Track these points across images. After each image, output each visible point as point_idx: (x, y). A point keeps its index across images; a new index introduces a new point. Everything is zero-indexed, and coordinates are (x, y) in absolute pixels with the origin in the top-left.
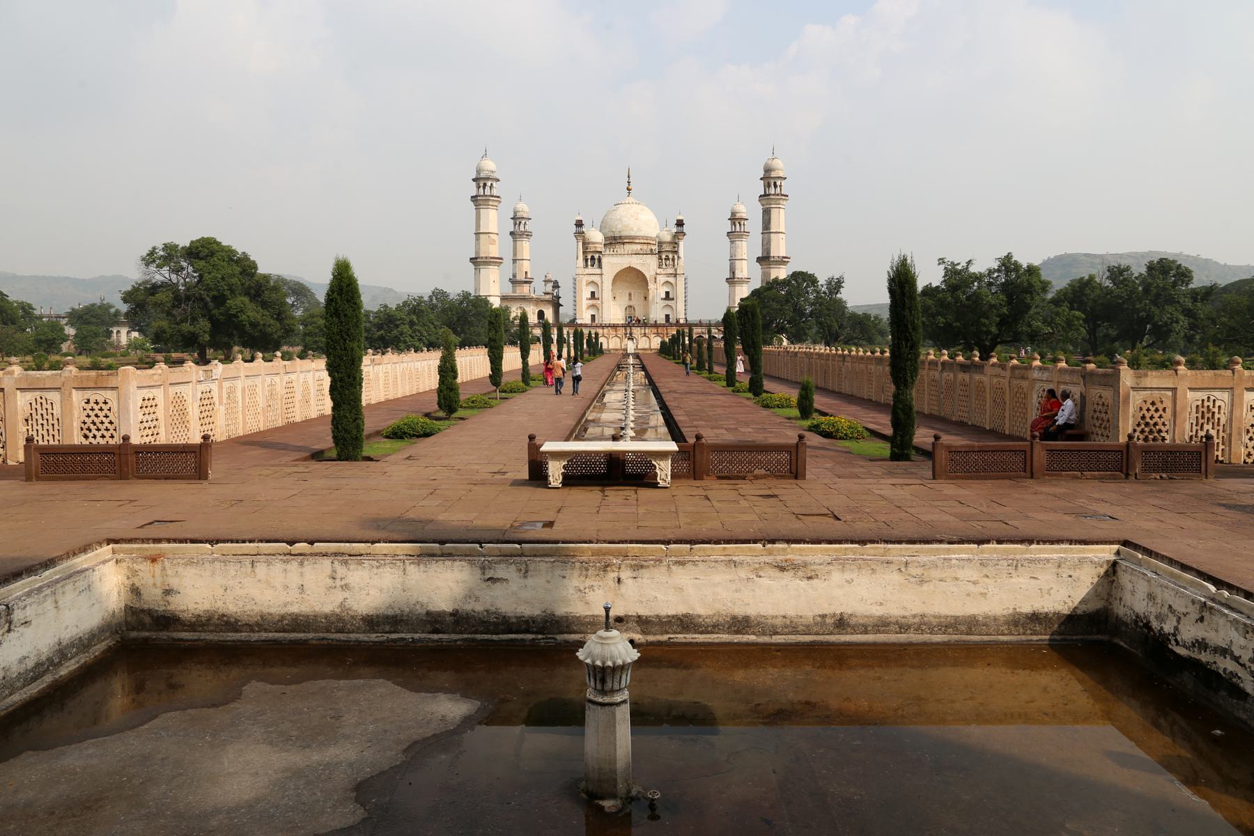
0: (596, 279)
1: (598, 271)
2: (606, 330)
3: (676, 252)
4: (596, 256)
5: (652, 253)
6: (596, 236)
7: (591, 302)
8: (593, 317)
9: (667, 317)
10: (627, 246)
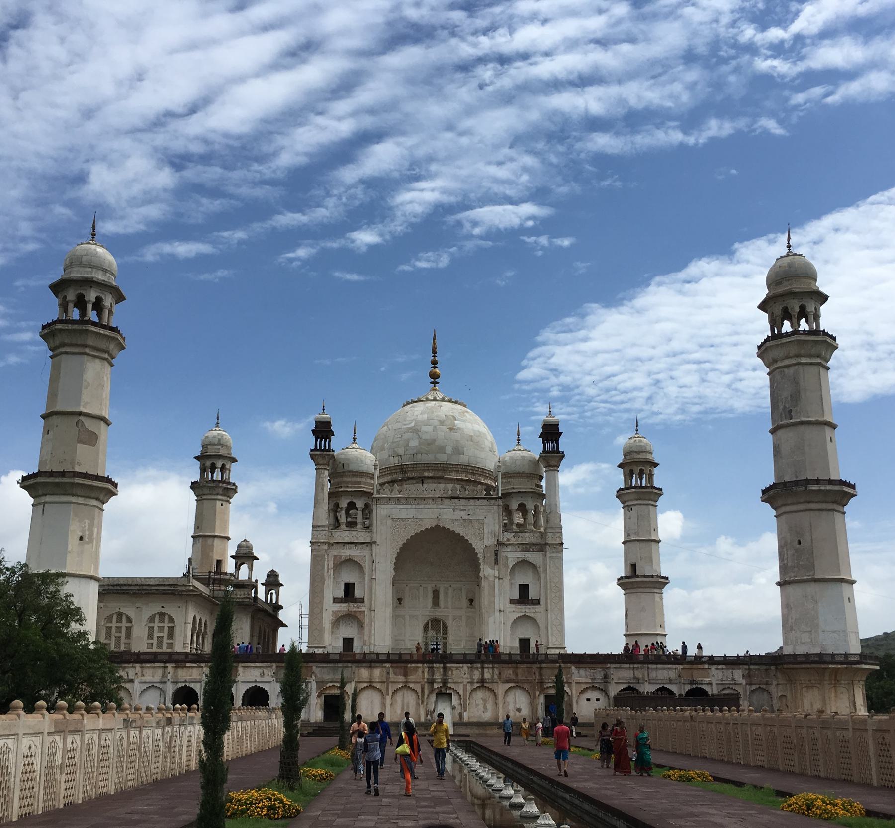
2: (377, 672)
3: (543, 496)
4: (360, 504)
5: (488, 498)
7: (343, 607)
8: (348, 643)
9: (524, 642)
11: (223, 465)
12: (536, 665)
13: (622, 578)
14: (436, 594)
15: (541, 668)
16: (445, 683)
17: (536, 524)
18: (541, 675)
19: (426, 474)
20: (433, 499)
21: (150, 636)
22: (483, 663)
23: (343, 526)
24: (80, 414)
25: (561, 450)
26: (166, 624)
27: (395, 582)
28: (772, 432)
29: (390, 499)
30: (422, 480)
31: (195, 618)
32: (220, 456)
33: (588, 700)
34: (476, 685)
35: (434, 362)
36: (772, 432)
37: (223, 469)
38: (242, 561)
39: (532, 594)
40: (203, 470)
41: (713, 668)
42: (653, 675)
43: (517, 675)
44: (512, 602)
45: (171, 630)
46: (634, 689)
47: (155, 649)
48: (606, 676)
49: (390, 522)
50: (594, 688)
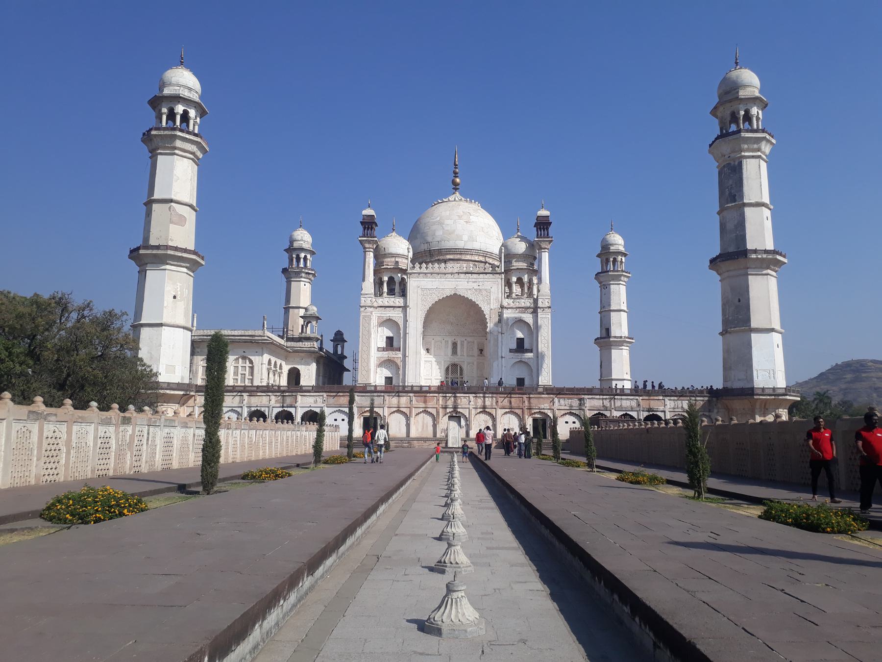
0: (397, 315)
1: (399, 301)
2: (404, 400)
3: (537, 272)
6: (399, 246)
8: (389, 380)
10: (450, 265)
11: (305, 256)
12: (525, 396)
13: (597, 339)
14: (455, 345)
15: (530, 398)
16: (455, 408)
17: (530, 295)
18: (529, 402)
19: (448, 257)
20: (452, 274)
21: (236, 373)
22: (484, 393)
23: (385, 295)
24: (171, 201)
25: (550, 235)
26: (248, 364)
27: (424, 335)
28: (719, 213)
29: (419, 273)
30: (445, 261)
31: (270, 361)
32: (302, 250)
33: (567, 422)
34: (479, 410)
35: (456, 174)
36: (719, 213)
37: (305, 258)
38: (309, 320)
39: (527, 345)
40: (291, 260)
41: (667, 399)
42: (618, 403)
43: (510, 403)
44: (511, 351)
45: (252, 368)
46: (602, 414)
47: (239, 384)
48: (580, 405)
49: (420, 291)
50: (571, 414)
